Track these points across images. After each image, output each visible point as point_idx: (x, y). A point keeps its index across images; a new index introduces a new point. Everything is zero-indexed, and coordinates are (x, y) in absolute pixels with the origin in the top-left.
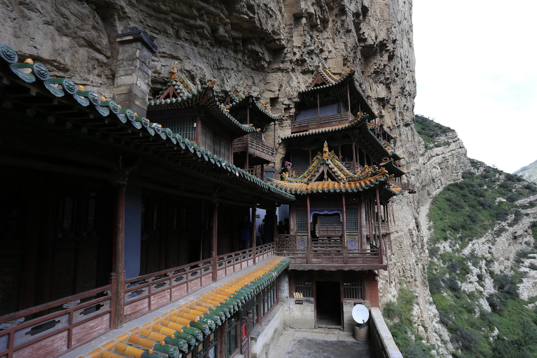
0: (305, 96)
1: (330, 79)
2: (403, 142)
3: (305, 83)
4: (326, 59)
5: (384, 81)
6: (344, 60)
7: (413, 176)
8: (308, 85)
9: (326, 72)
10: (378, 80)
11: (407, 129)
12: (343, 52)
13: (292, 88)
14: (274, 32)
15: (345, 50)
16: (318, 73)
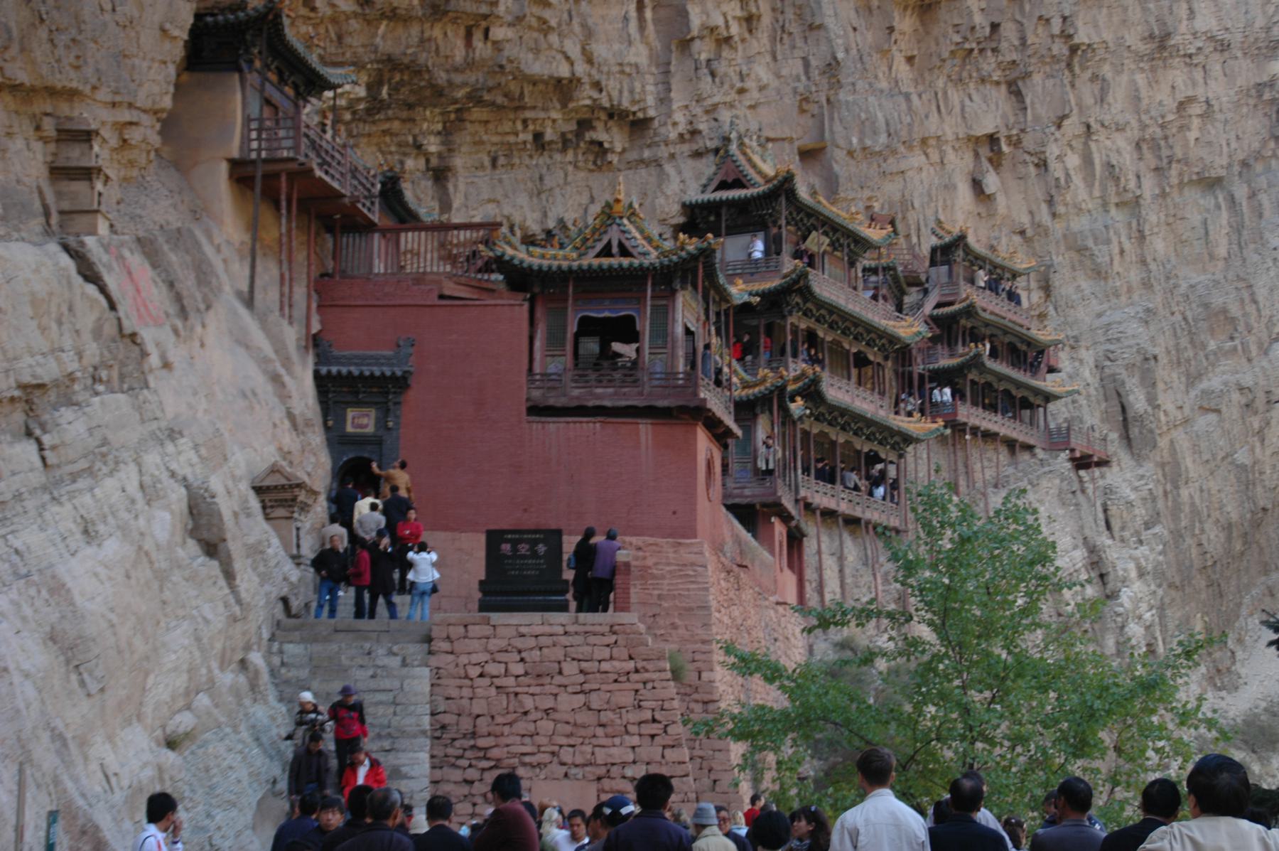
0: (697, 211)
1: (752, 173)
2: (1153, 266)
3: (698, 178)
4: (752, 107)
5: (999, 73)
6: (801, 101)
7: (1212, 417)
8: (704, 181)
9: (745, 154)
10: (971, 77)
11: (1208, 202)
12: (797, 84)
13: (667, 197)
14: (634, 102)
15: (803, 78)
16: (727, 155)
